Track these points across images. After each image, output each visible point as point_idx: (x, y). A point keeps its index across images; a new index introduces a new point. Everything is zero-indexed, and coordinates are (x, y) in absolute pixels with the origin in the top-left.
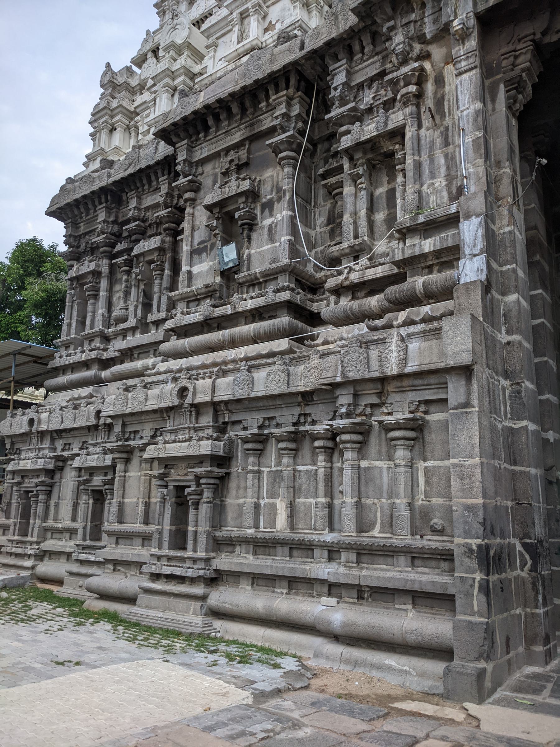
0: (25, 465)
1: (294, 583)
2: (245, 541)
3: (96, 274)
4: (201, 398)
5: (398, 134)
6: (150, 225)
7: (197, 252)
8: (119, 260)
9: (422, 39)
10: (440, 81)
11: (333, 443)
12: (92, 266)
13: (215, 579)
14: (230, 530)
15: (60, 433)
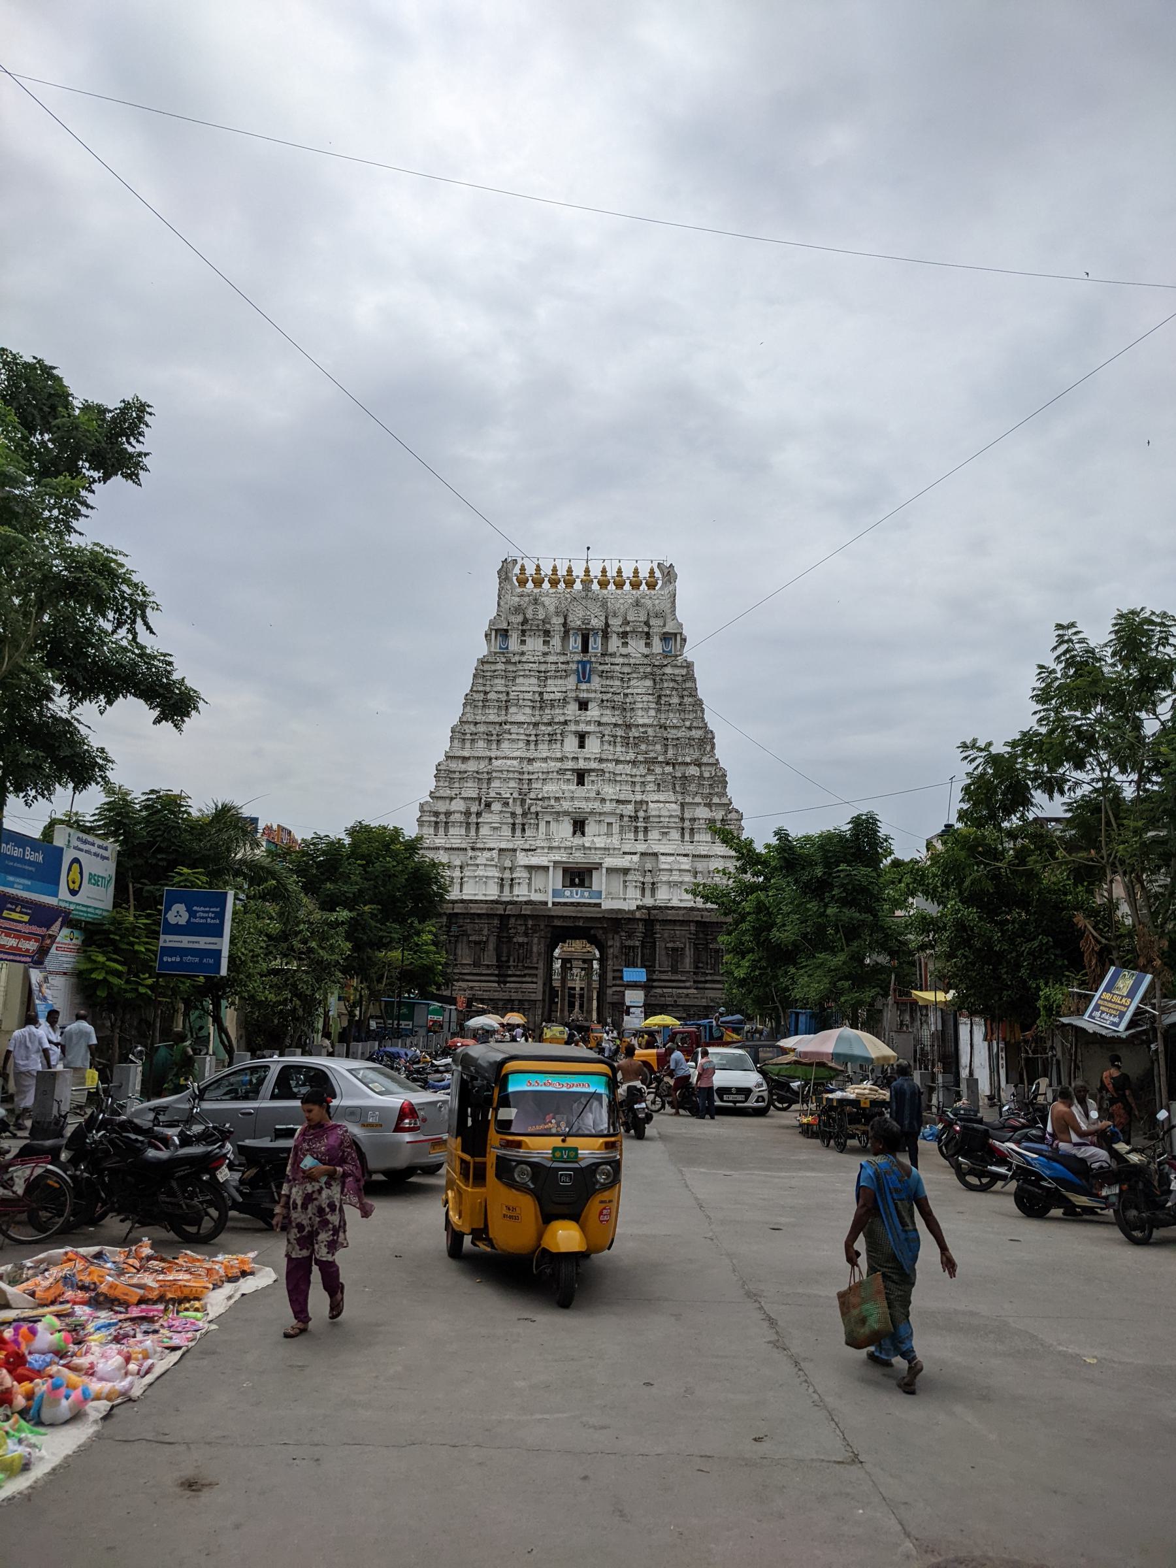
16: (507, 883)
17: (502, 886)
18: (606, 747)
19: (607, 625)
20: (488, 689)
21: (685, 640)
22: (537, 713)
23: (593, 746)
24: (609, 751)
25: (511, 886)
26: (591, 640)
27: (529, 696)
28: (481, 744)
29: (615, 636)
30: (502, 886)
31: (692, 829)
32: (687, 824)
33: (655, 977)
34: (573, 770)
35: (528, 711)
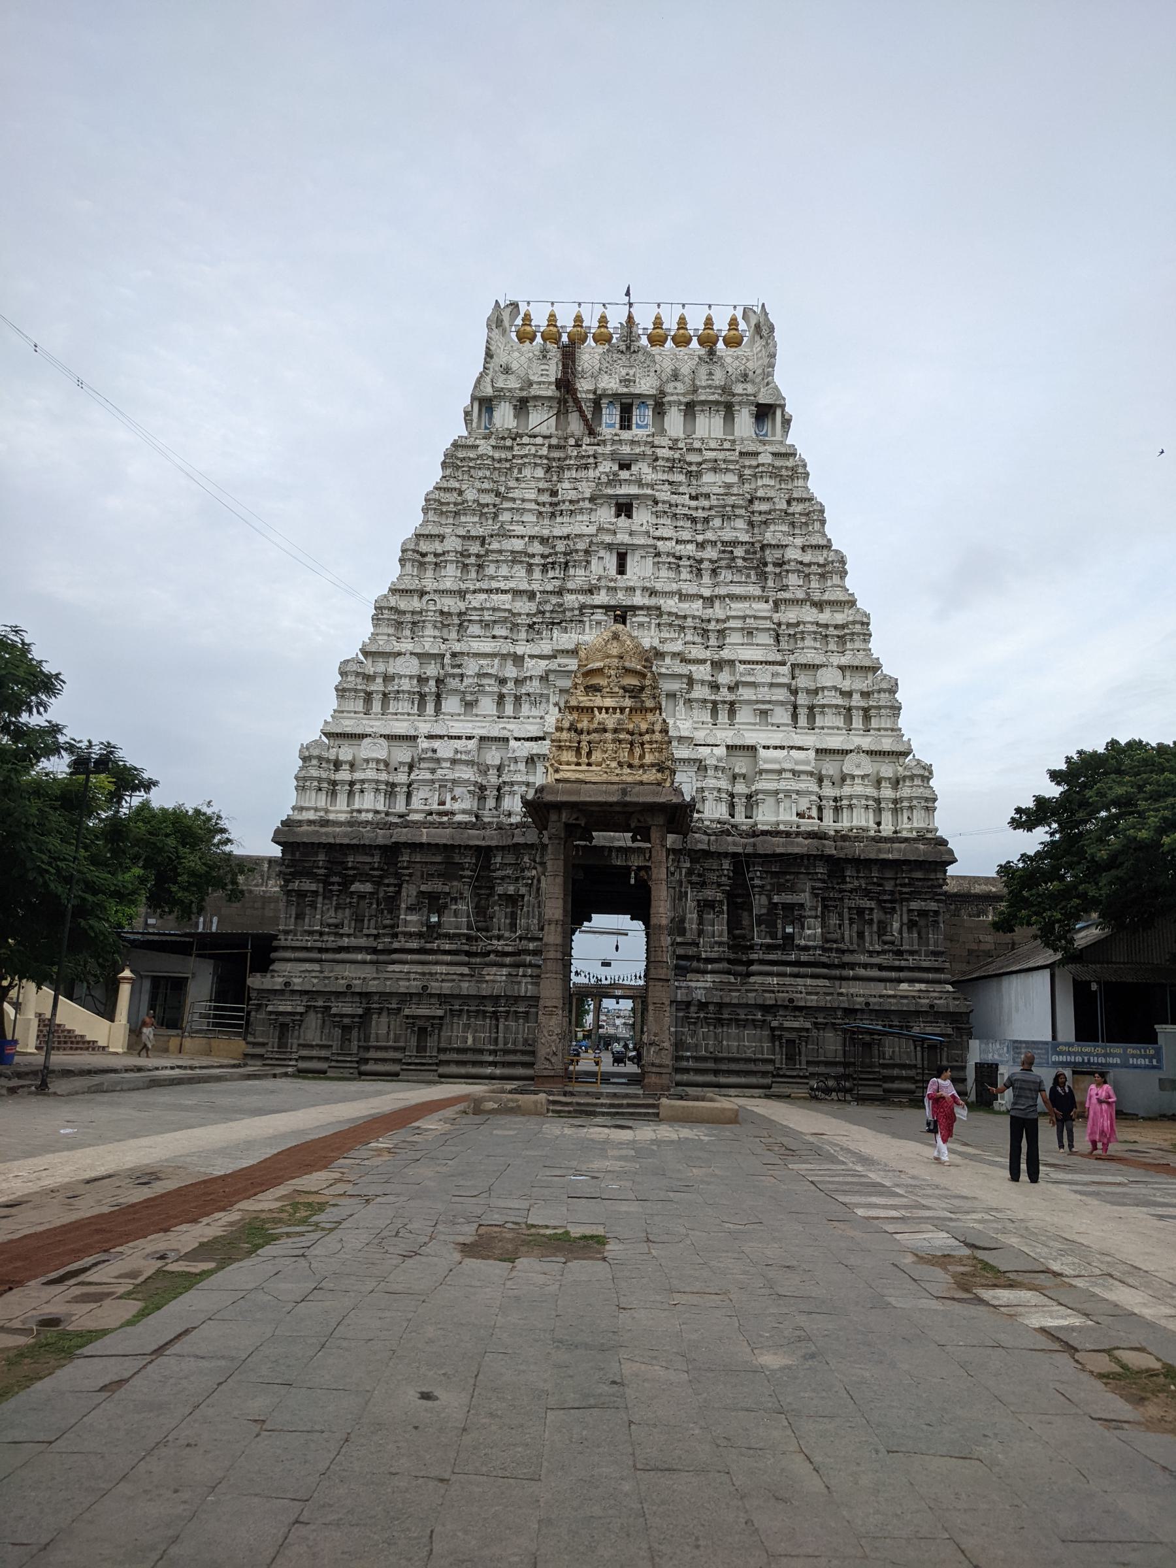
0: (281, 1009)
1: (475, 1063)
2: (454, 1049)
3: (315, 893)
4: (434, 991)
5: (523, 896)
6: (361, 874)
7: (410, 909)
8: (336, 888)
9: (535, 861)
10: (539, 881)
11: (495, 1016)
12: (313, 887)
13: (441, 1063)
14: (442, 1045)
15: (306, 992)
16: (491, 793)
17: (482, 798)
18: (664, 573)
19: (663, 393)
20: (464, 487)
21: (787, 422)
22: (546, 522)
23: (639, 570)
24: (664, 580)
25: (498, 799)
26: (635, 412)
27: (532, 495)
28: (451, 570)
29: (674, 410)
30: (482, 798)
31: (811, 708)
32: (802, 699)
33: (755, 956)
34: (607, 608)
35: (530, 518)
